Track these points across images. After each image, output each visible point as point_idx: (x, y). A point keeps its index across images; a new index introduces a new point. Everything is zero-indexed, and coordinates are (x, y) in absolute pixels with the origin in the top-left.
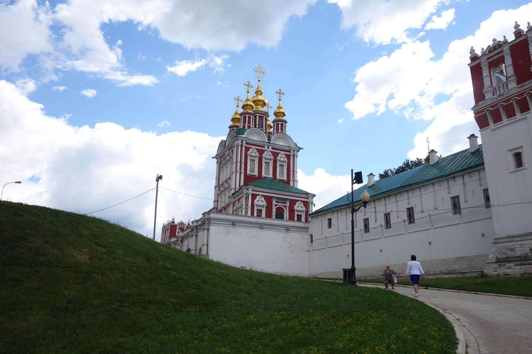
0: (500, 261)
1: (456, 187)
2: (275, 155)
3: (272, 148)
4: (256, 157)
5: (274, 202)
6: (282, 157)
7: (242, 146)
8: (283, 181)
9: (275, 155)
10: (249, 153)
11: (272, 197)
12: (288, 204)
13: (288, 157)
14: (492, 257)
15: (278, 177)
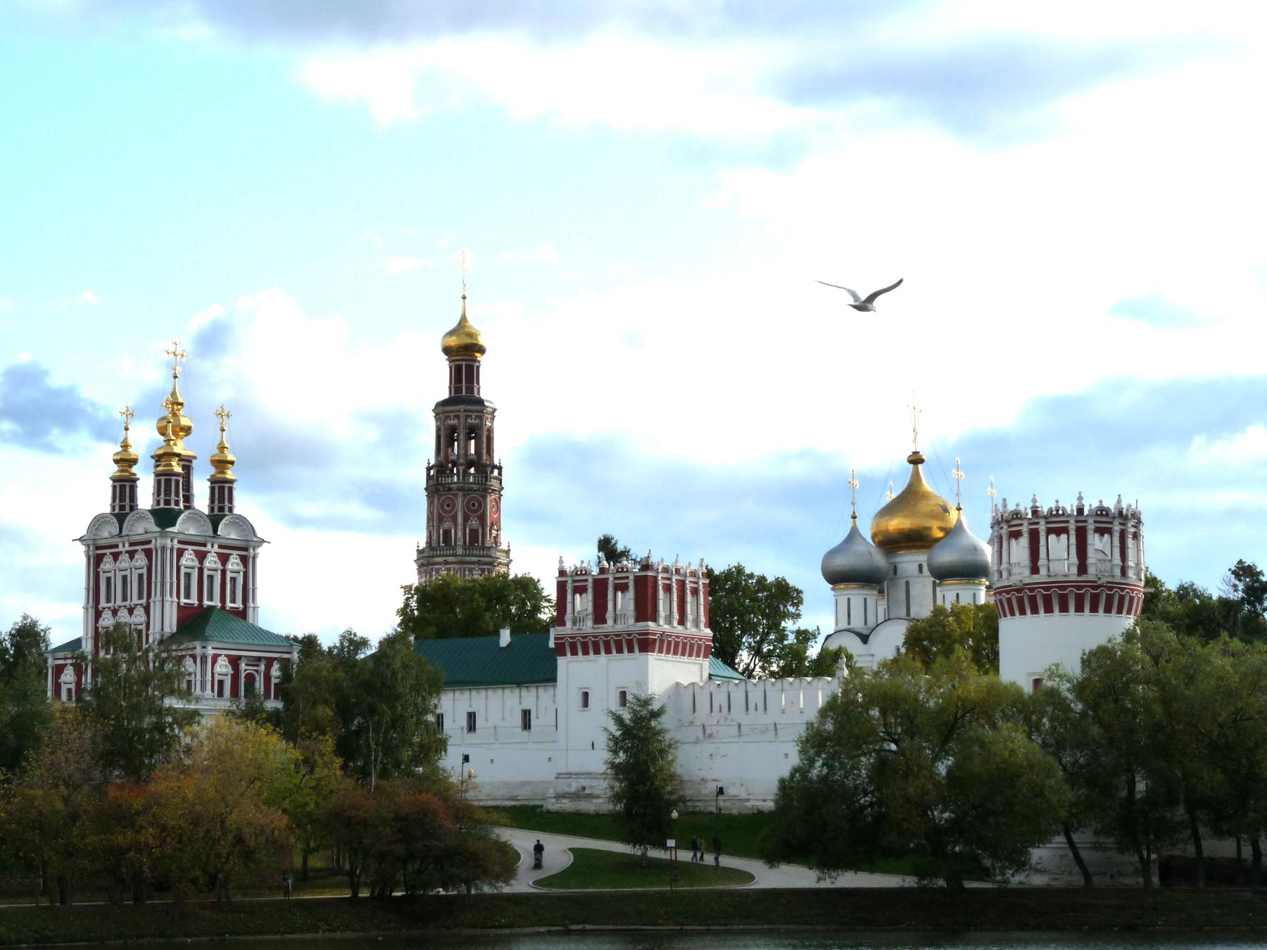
0: (559, 797)
1: (528, 697)
2: (224, 559)
3: (220, 547)
4: (193, 568)
5: (243, 666)
6: (234, 563)
7: (172, 550)
8: (234, 612)
9: (224, 559)
10: (183, 562)
11: (239, 658)
12: (262, 667)
13: (244, 560)
14: (551, 792)
15: (229, 605)
